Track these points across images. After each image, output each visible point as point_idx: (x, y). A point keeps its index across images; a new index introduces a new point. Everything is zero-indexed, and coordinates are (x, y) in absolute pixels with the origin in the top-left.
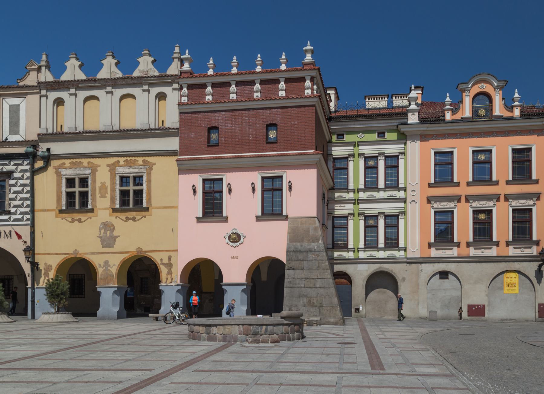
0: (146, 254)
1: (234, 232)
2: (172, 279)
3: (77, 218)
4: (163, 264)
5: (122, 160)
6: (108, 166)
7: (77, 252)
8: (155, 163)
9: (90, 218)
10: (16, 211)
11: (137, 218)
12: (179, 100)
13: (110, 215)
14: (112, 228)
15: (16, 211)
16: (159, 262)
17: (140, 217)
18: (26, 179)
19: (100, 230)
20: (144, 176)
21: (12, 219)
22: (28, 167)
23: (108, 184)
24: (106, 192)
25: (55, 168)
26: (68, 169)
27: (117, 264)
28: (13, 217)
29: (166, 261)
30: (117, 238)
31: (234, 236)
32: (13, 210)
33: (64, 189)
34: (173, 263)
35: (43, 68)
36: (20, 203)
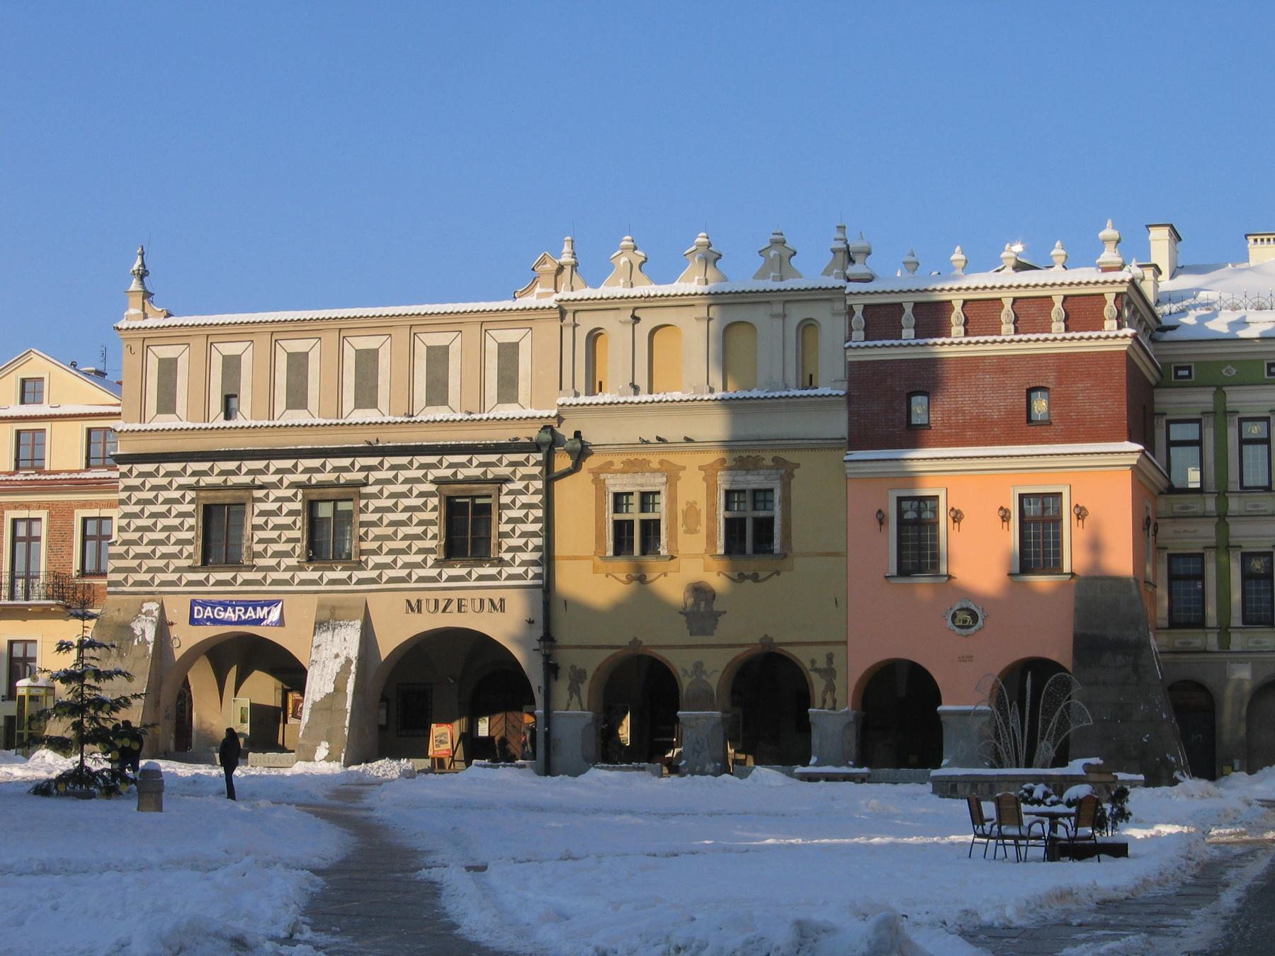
1: (965, 606)
2: (835, 701)
4: (816, 670)
6: (701, 468)
8: (799, 464)
9: (665, 574)
10: (513, 559)
11: (762, 575)
12: (847, 335)
13: (706, 569)
15: (513, 559)
16: (808, 665)
17: (766, 574)
18: (534, 493)
20: (775, 491)
21: (504, 575)
22: (537, 470)
23: (702, 506)
24: (698, 523)
26: (618, 475)
27: (721, 670)
28: (507, 571)
29: (821, 664)
30: (720, 615)
31: (963, 616)
33: (610, 516)
34: (836, 669)
35: (567, 270)
36: (521, 542)
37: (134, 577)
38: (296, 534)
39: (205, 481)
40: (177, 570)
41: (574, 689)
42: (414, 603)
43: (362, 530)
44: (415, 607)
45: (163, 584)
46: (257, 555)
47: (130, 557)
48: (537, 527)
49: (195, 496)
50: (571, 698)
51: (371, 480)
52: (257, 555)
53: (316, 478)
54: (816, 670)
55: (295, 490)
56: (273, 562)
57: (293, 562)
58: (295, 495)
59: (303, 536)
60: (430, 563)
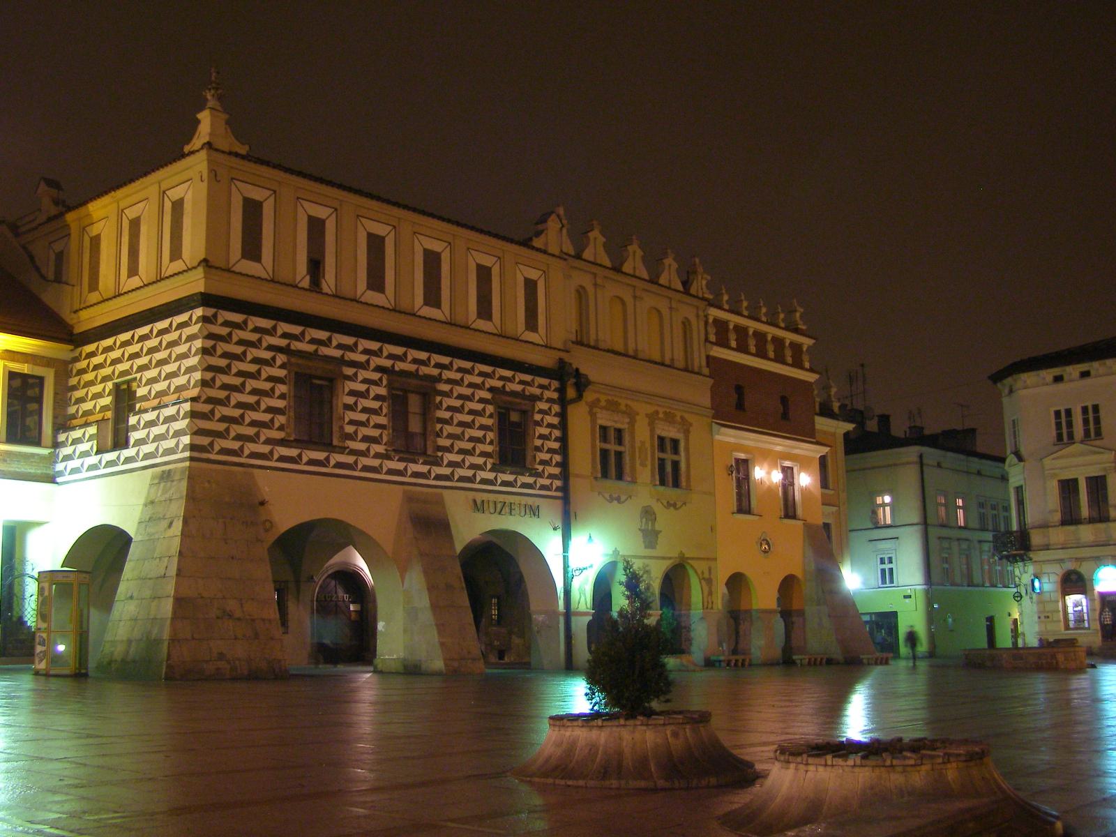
3: (617, 495)
6: (647, 415)
11: (679, 504)
19: (642, 519)
22: (555, 396)
23: (648, 445)
38: (382, 420)
39: (297, 345)
40: (268, 441)
42: (479, 502)
43: (439, 426)
45: (253, 455)
48: (556, 445)
49: (286, 360)
51: (444, 377)
52: (352, 437)
53: (400, 366)
56: (362, 446)
57: (380, 449)
58: (381, 379)
59: (389, 423)
60: (489, 466)
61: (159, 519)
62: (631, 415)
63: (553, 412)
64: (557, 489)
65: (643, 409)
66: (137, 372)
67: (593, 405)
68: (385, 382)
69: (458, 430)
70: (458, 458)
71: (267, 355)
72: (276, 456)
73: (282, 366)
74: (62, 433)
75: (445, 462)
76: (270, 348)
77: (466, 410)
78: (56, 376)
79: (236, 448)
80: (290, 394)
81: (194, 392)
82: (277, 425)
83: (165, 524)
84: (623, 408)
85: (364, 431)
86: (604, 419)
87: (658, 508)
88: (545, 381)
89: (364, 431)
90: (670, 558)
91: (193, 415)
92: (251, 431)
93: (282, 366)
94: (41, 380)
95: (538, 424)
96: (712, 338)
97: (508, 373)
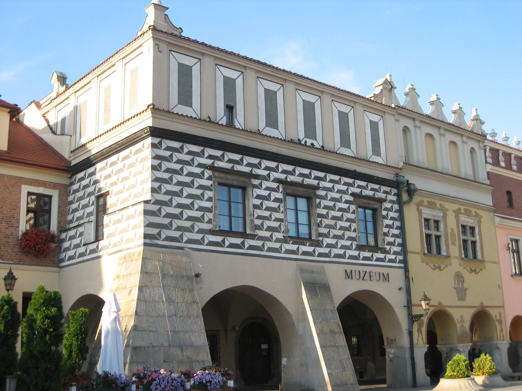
0: (486, 310)
5: (462, 208)
6: (454, 211)
7: (441, 305)
9: (447, 266)
11: (478, 270)
14: (462, 279)
16: (495, 319)
19: (455, 281)
22: (395, 198)
23: (456, 231)
24: (455, 240)
25: (417, 205)
29: (498, 318)
32: (388, 247)
37: (165, 233)
40: (200, 231)
41: (420, 331)
42: (349, 272)
43: (319, 220)
44: (349, 275)
46: (258, 228)
47: (162, 215)
48: (397, 232)
50: (419, 336)
51: (321, 185)
52: (258, 228)
53: (291, 178)
54: (497, 320)
55: (277, 184)
56: (267, 234)
57: (280, 236)
58: (278, 187)
60: (354, 247)
61: (123, 288)
62: (444, 211)
63: (394, 210)
64: (400, 262)
65: (451, 207)
66: (109, 187)
67: (420, 204)
68: (281, 189)
69: (333, 222)
70: (333, 241)
71: (198, 170)
72: (206, 242)
73: (209, 178)
74: (63, 233)
75: (325, 244)
76: (200, 165)
77: (337, 208)
78: (60, 195)
79: (178, 236)
80: (215, 198)
81: (148, 196)
82: (206, 219)
83: (127, 291)
84: (438, 206)
85: (267, 223)
86: (427, 213)
87: (465, 273)
88: (388, 189)
89: (267, 223)
90: (475, 307)
91: (146, 212)
92: (188, 224)
93: (209, 178)
94: (50, 197)
95: (385, 217)
96: (490, 160)
97: (363, 184)
